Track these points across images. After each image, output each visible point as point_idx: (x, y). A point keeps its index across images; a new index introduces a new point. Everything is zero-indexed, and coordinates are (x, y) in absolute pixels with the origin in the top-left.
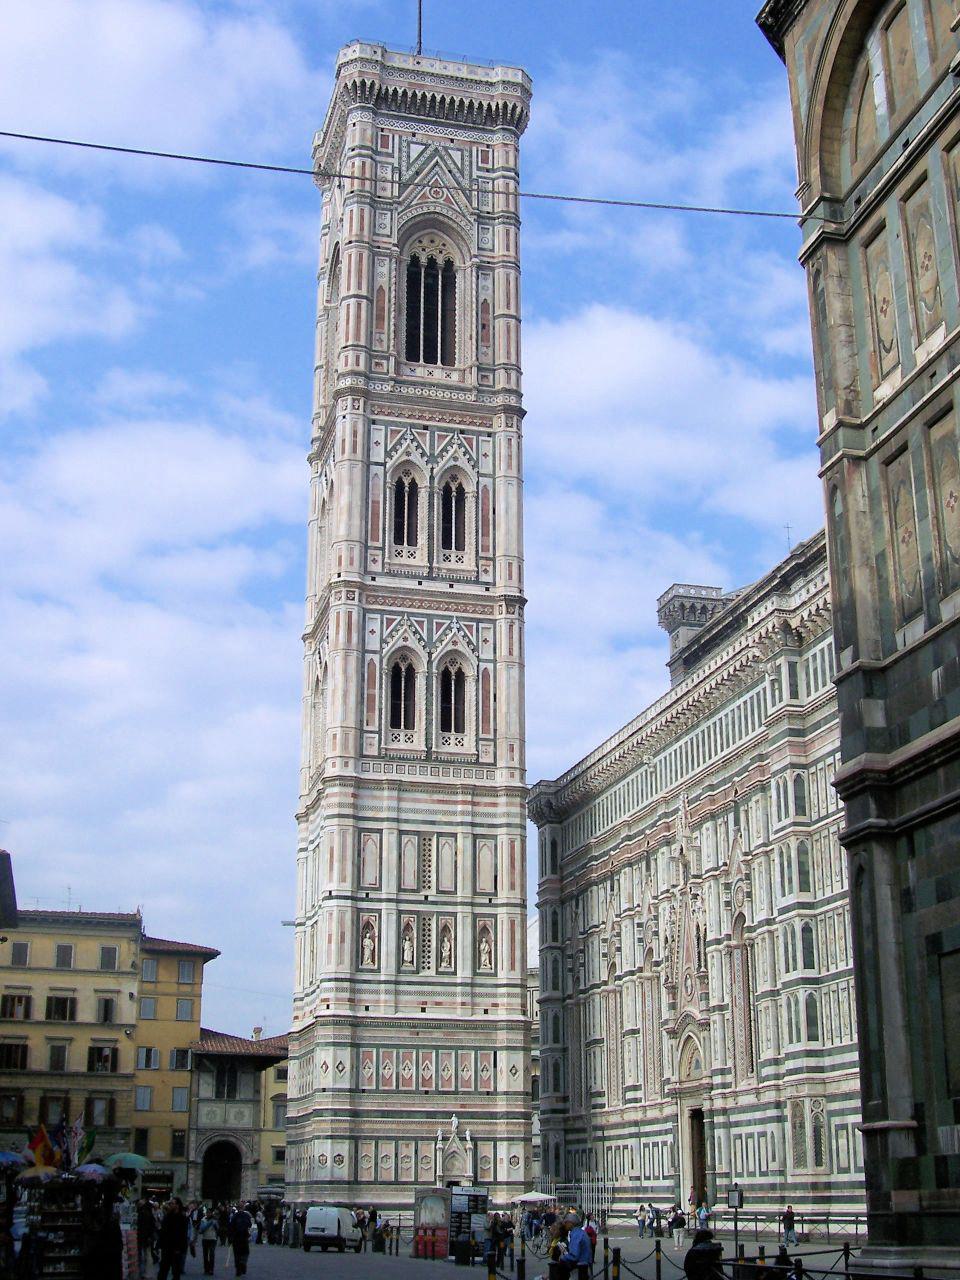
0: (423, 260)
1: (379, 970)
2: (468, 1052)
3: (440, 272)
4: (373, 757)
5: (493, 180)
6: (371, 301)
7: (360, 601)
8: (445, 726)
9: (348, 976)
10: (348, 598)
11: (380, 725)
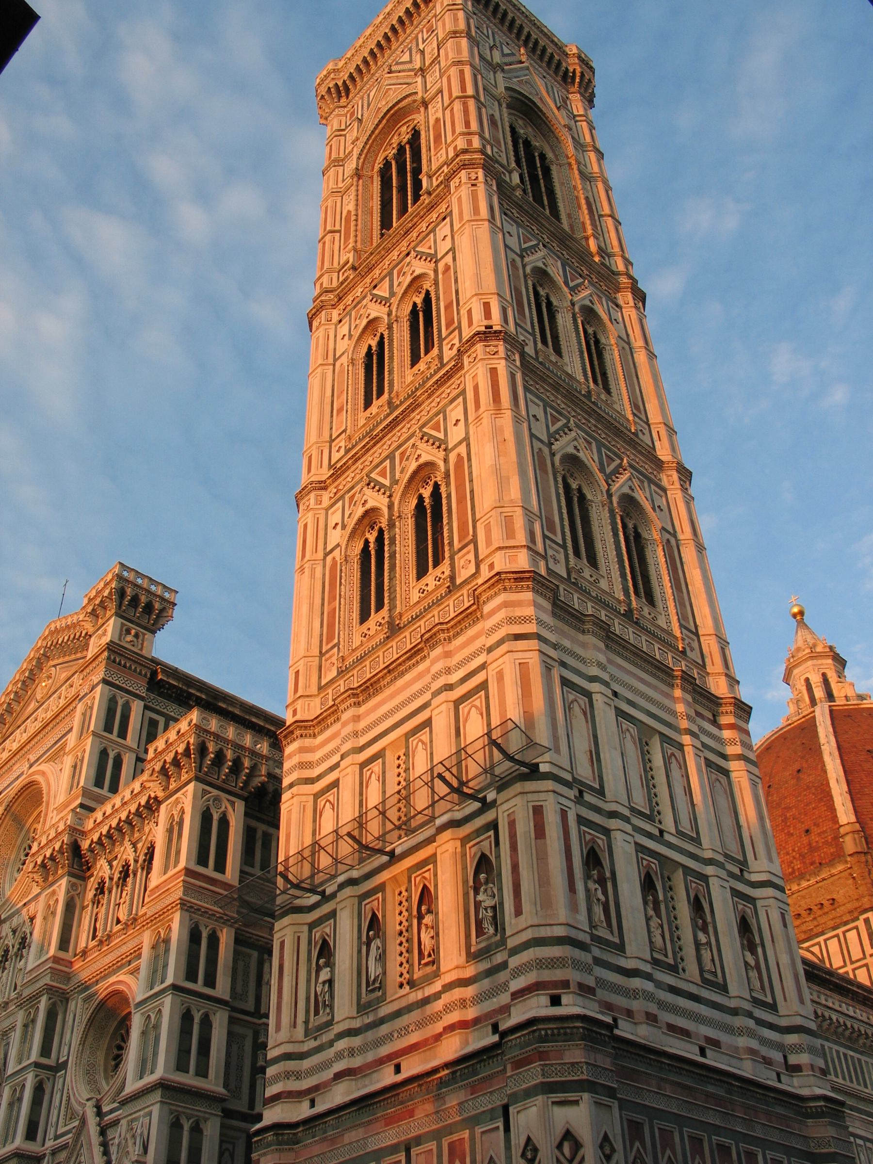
3: (407, 147)
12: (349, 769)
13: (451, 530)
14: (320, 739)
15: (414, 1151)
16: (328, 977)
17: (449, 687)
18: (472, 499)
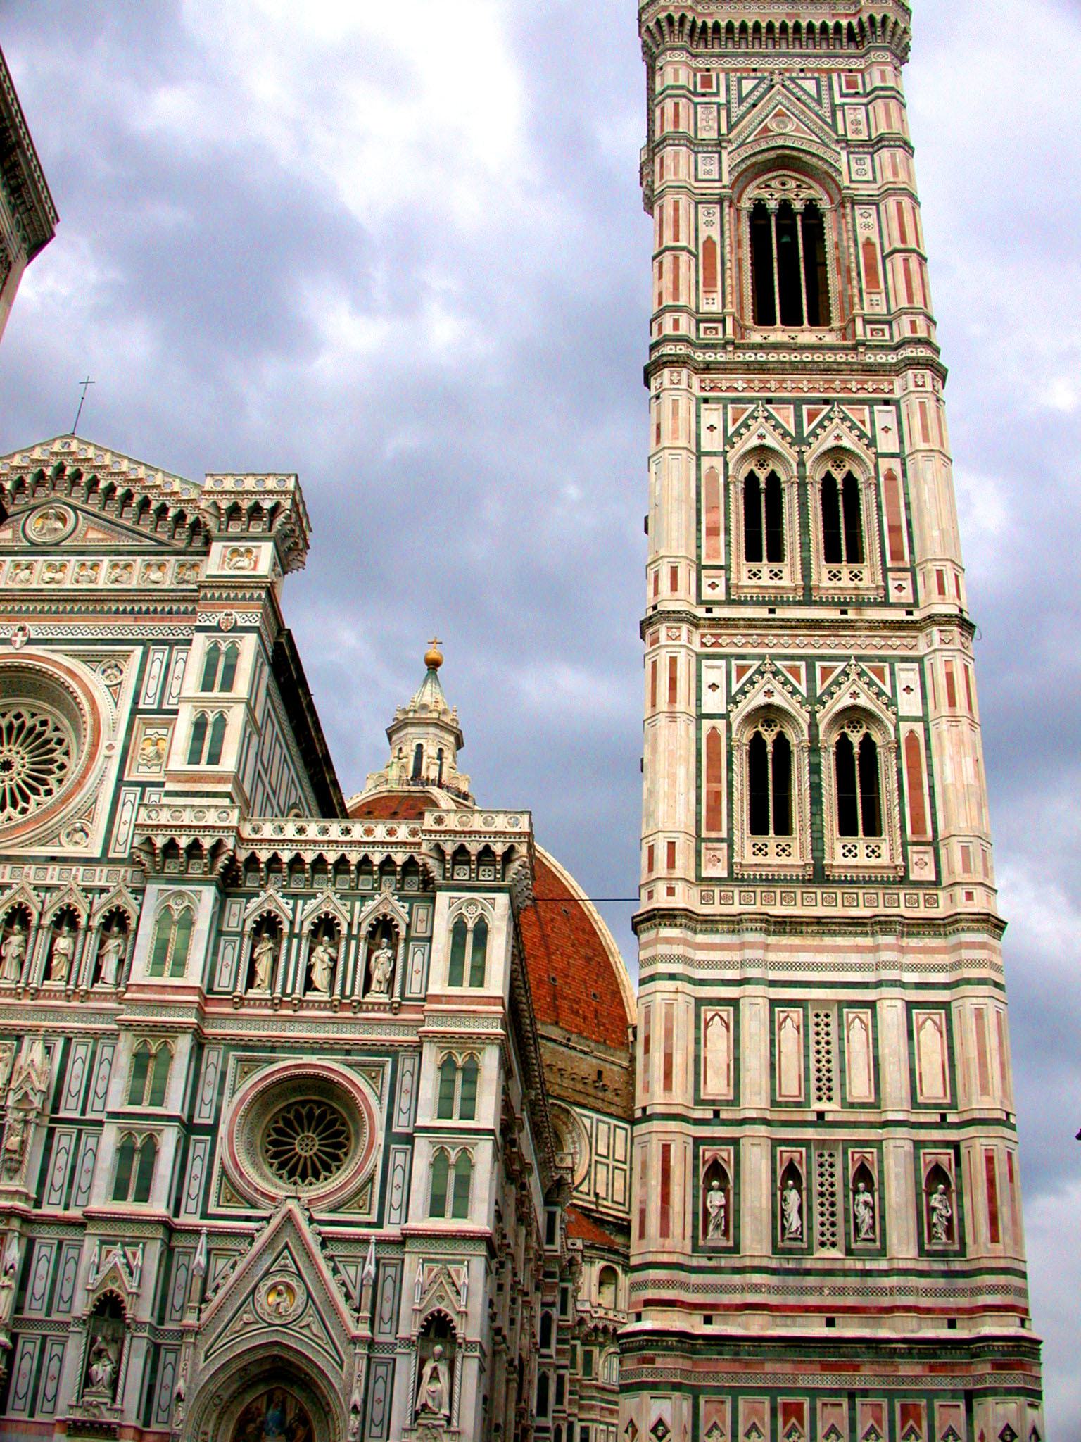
0: (772, 205)
1: (736, 1249)
2: (917, 1401)
3: (799, 218)
4: (718, 881)
5: (866, 105)
6: (696, 257)
7: (690, 641)
8: (847, 828)
9: (674, 1258)
10: (669, 637)
11: (730, 829)
12: (760, 1000)
13: (902, 813)
14: (700, 938)
15: (858, 1401)
16: (723, 1202)
17: (902, 985)
18: (932, 796)
